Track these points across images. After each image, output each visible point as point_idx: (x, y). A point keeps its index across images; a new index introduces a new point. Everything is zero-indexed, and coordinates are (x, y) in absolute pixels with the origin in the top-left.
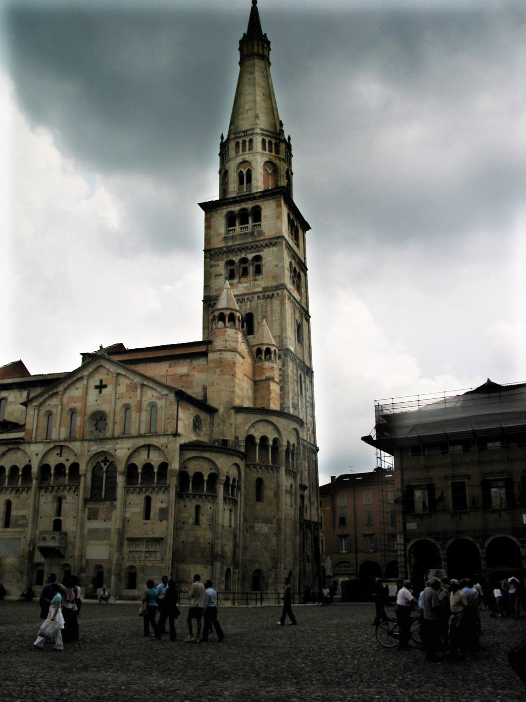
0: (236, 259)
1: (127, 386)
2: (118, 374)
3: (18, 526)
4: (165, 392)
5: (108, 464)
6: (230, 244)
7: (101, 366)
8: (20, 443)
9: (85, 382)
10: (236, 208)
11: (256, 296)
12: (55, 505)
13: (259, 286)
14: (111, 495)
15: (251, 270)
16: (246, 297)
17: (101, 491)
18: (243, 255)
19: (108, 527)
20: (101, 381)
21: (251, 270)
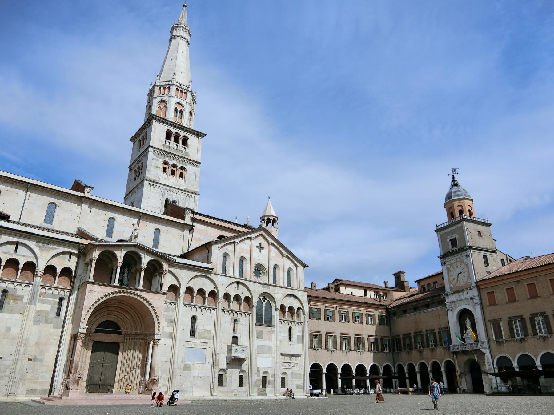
0: (171, 162)
1: (276, 253)
2: (273, 244)
3: (203, 338)
4: (298, 264)
5: (266, 301)
6: (167, 150)
7: (262, 235)
8: (210, 273)
9: (252, 241)
10: (174, 131)
11: (181, 192)
12: (233, 324)
13: (182, 186)
14: (269, 323)
15: (177, 173)
16: (174, 190)
17: (264, 320)
18: (175, 162)
19: (270, 345)
20: (260, 244)
21: (177, 173)
